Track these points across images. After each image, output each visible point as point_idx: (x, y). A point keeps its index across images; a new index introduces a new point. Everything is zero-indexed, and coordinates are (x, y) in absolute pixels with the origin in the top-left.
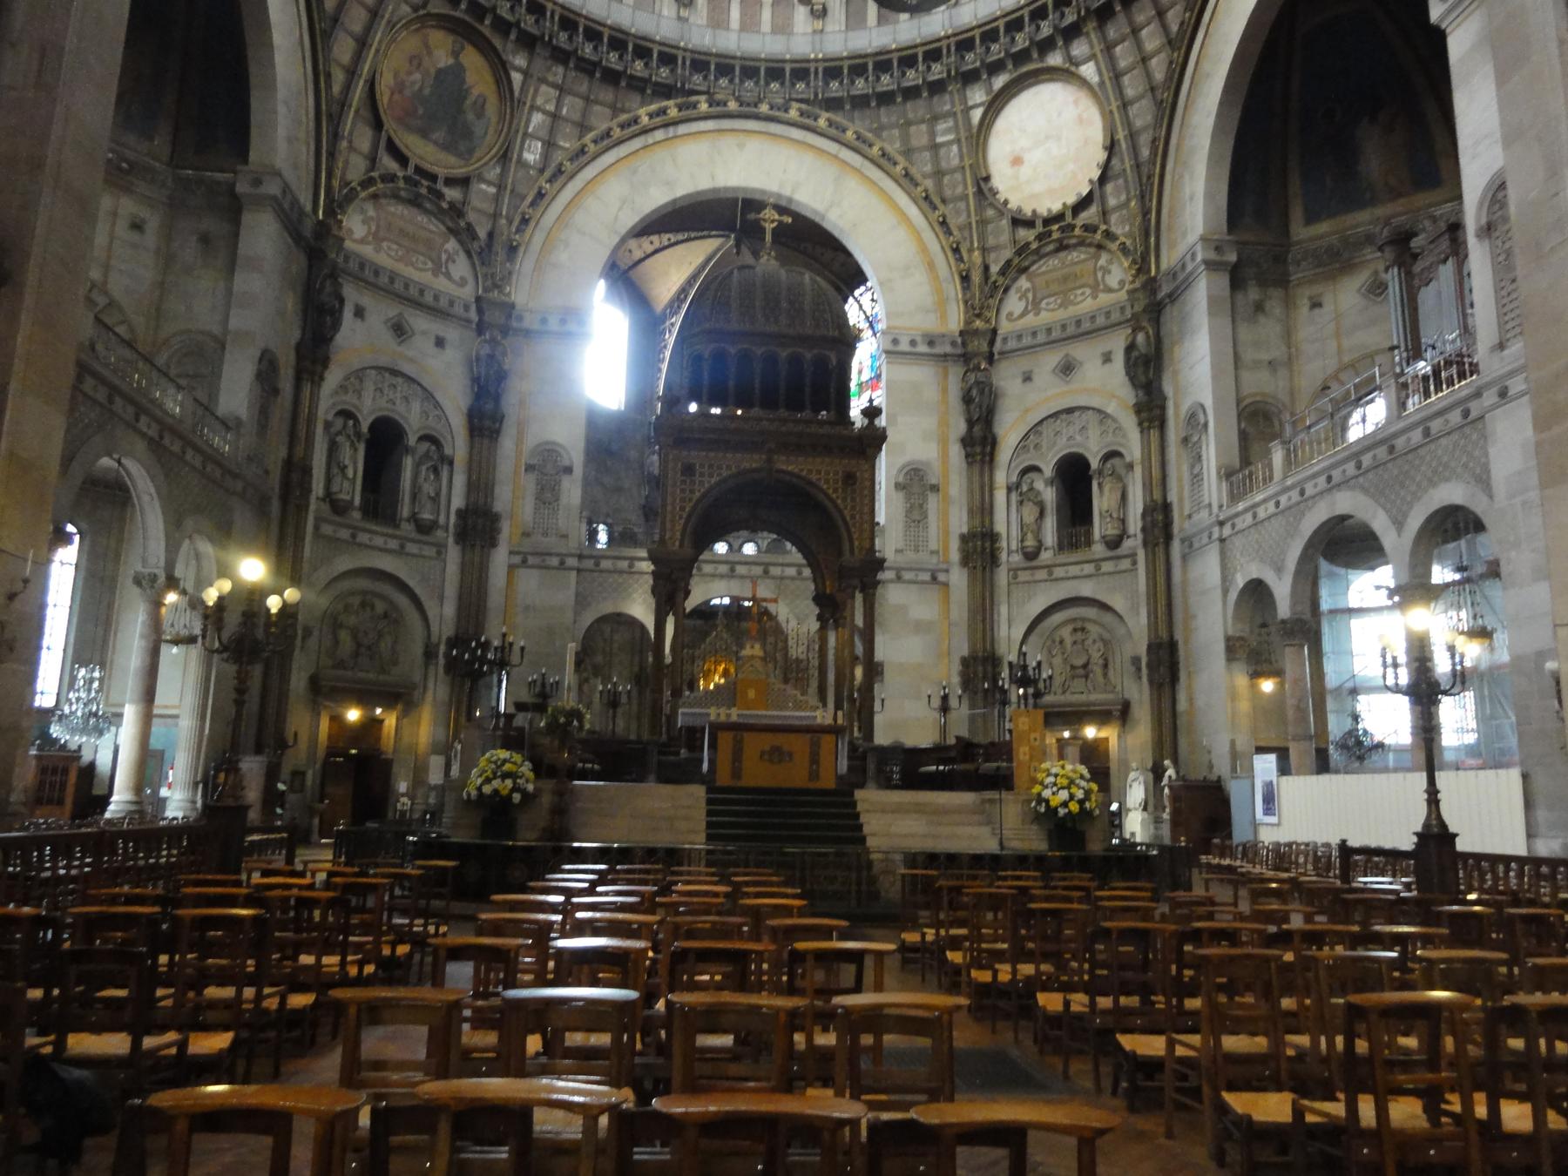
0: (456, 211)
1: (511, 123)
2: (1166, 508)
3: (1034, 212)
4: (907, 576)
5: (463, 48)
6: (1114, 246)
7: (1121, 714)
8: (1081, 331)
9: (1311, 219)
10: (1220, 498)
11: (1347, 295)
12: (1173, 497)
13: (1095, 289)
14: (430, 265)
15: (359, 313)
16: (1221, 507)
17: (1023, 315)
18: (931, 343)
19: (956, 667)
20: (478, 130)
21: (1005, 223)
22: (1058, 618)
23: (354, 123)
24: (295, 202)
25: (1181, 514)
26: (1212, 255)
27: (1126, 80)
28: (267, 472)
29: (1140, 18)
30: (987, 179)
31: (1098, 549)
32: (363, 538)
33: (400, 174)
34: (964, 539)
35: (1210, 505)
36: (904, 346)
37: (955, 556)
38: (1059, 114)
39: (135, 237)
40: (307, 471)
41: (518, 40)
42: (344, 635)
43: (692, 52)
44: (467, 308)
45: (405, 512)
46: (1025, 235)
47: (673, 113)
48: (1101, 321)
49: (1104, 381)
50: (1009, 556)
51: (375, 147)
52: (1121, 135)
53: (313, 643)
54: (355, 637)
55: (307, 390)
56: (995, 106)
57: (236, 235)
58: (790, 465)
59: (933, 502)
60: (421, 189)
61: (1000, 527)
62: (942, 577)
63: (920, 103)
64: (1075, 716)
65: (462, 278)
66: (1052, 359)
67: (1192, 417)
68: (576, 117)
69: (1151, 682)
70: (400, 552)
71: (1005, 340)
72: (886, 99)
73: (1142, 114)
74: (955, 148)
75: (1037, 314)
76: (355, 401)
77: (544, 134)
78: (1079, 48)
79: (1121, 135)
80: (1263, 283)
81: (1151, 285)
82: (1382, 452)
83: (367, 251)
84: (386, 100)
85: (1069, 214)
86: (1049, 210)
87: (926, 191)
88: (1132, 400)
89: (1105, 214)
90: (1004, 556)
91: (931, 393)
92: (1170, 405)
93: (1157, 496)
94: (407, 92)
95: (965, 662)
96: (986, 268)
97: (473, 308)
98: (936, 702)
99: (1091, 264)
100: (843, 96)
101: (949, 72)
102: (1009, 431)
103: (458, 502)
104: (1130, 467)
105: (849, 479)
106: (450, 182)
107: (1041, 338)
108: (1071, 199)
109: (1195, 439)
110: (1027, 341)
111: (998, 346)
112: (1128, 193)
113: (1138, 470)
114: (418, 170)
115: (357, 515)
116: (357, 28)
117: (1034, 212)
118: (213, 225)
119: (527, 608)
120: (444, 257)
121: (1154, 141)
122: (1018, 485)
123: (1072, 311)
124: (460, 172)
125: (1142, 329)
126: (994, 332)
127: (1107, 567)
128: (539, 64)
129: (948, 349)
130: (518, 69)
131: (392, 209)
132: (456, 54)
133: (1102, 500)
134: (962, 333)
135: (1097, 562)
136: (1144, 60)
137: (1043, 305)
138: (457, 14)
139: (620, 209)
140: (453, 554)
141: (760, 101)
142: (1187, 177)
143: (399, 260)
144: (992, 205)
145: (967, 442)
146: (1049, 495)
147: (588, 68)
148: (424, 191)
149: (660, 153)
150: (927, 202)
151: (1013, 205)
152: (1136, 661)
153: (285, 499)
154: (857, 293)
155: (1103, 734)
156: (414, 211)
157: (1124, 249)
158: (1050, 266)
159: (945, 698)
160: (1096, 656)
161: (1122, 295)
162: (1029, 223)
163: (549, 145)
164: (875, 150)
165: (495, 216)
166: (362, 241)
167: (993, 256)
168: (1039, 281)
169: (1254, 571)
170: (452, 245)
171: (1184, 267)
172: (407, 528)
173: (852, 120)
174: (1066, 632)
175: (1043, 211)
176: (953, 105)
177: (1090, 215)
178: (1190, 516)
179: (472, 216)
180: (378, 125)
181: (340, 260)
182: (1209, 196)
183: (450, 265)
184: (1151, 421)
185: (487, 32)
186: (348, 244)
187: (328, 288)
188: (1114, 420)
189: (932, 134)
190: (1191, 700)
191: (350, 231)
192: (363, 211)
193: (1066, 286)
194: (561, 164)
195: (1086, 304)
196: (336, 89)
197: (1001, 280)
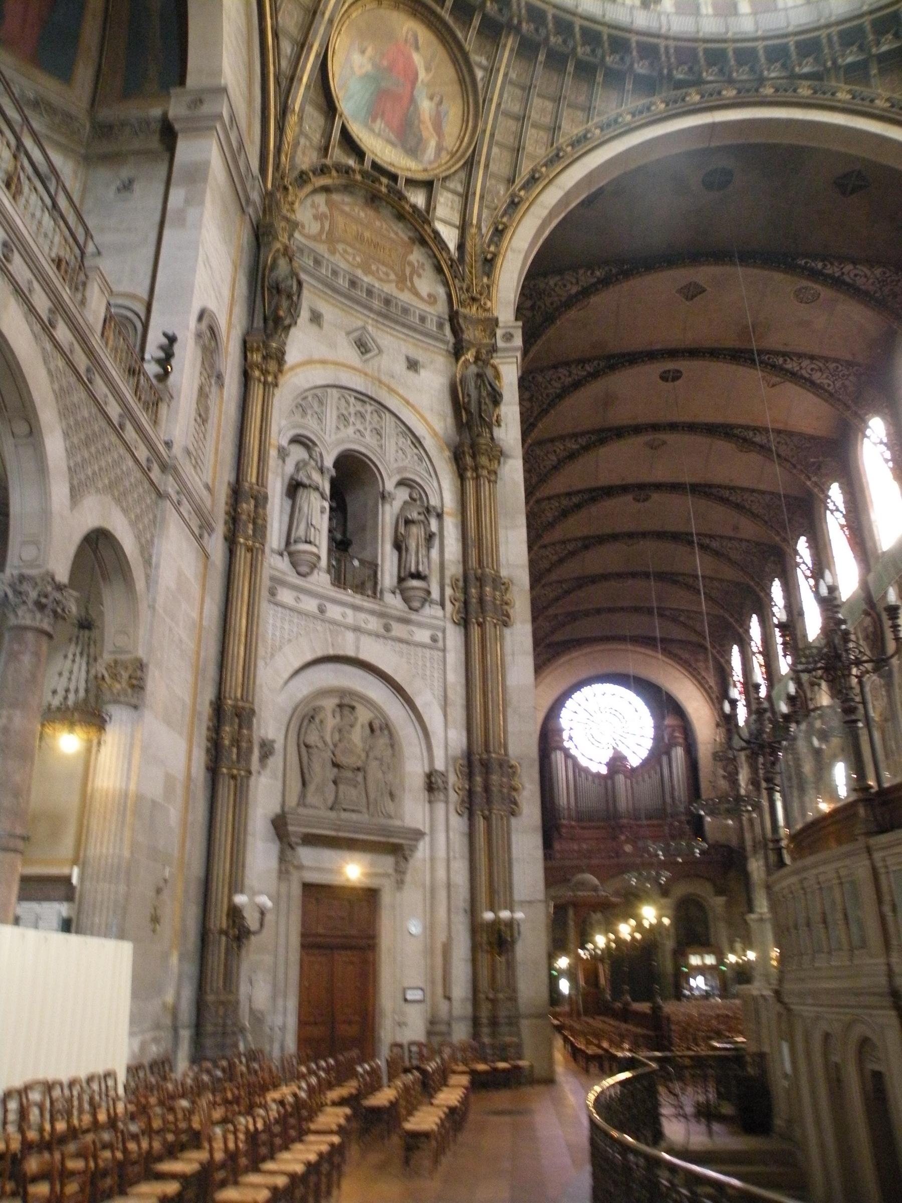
14: (393, 277)
15: (316, 318)
40: (261, 500)
43: (675, 39)
44: (440, 326)
55: (257, 391)
103: (454, 569)
114: (375, 165)
120: (408, 270)
130: (480, 66)
140: (454, 638)
143: (358, 266)
148: (384, 190)
183: (415, 278)
185: (447, 17)
186: (297, 235)
194: (534, 171)
196: (284, 64)
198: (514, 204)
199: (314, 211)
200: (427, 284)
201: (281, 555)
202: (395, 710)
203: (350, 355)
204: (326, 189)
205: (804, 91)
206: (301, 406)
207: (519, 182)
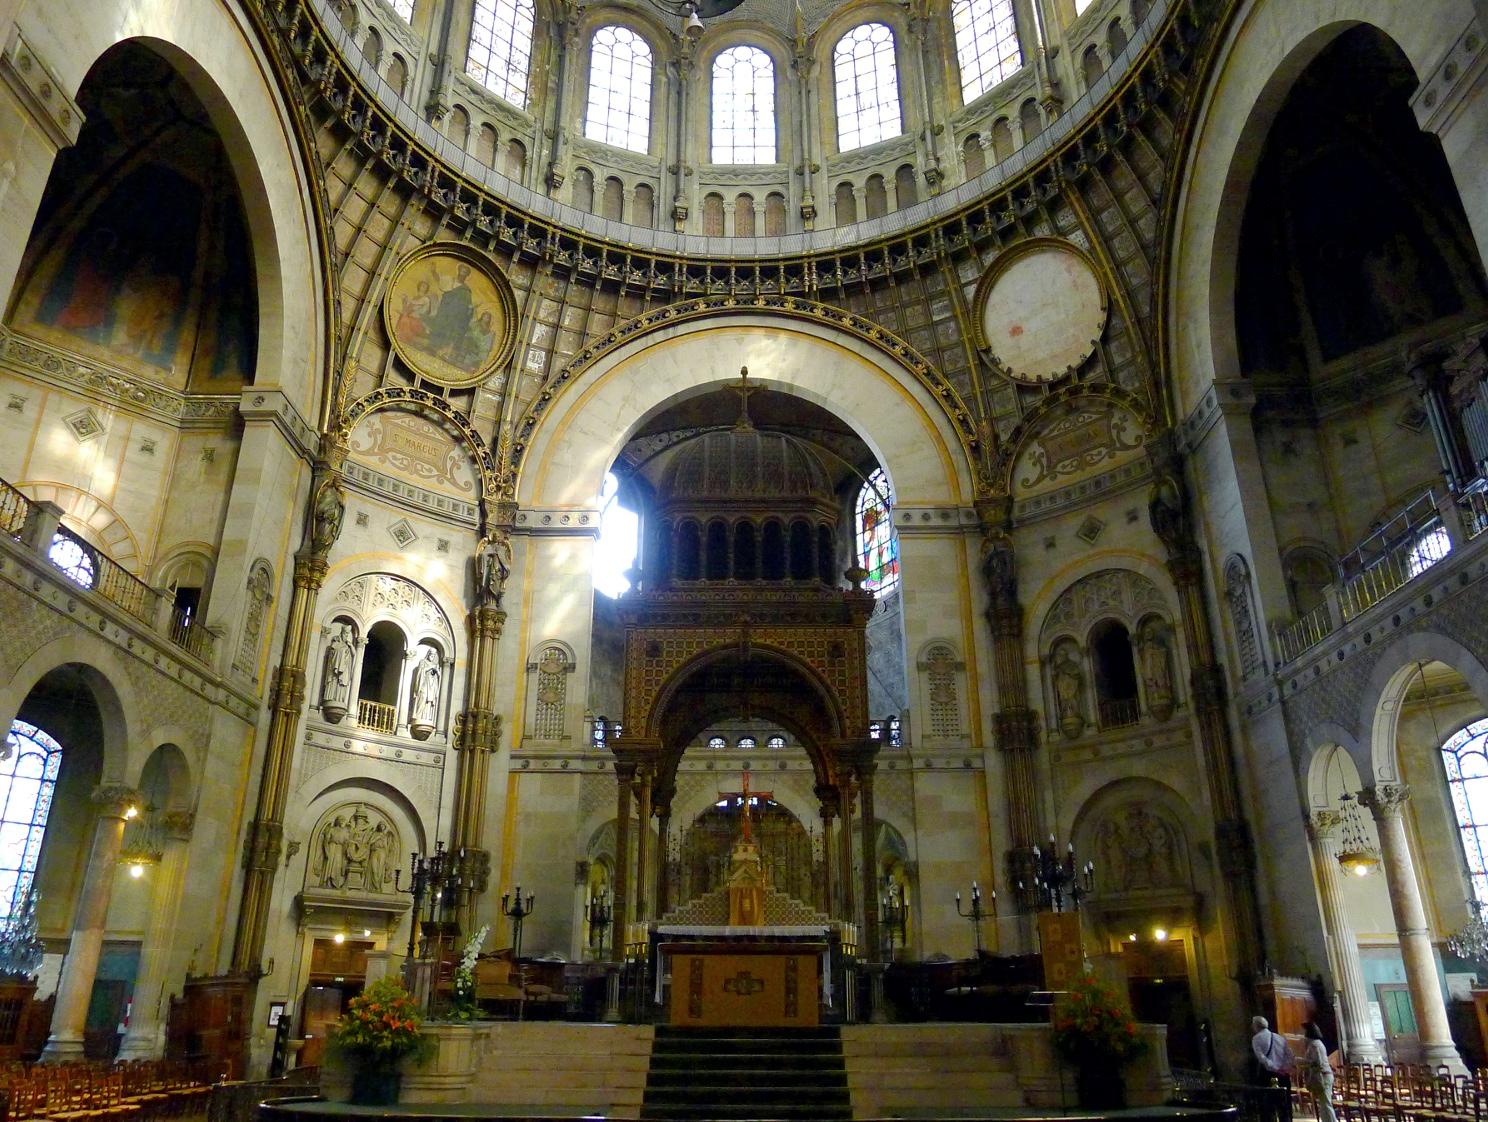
0: (462, 420)
1: (515, 335)
2: (1216, 670)
3: (1039, 377)
4: (938, 763)
5: (468, 273)
6: (1126, 403)
8: (1102, 490)
9: (1327, 358)
10: (1275, 655)
11: (1383, 428)
12: (1223, 659)
13: (1111, 447)
14: (435, 472)
15: (362, 520)
16: (1277, 665)
17: (1039, 480)
18: (945, 516)
19: (1000, 865)
20: (484, 345)
21: (1011, 391)
23: (362, 343)
24: (297, 417)
25: (1233, 675)
26: (1230, 399)
27: (1116, 243)
28: (254, 680)
29: (1122, 184)
30: (988, 350)
31: (1146, 721)
33: (407, 389)
34: (999, 719)
35: (1265, 662)
36: (917, 521)
37: (989, 738)
38: (1054, 282)
39: (145, 457)
40: (298, 677)
41: (520, 262)
42: (335, 852)
44: (470, 511)
46: (1030, 400)
47: (673, 315)
49: (1132, 540)
50: (1048, 737)
51: (383, 368)
52: (1118, 295)
53: (299, 859)
54: (345, 854)
55: (303, 594)
56: (987, 282)
57: (236, 452)
58: (766, 639)
59: (961, 682)
60: (427, 400)
61: (1037, 704)
62: (977, 763)
65: (466, 483)
66: (1074, 522)
67: (1232, 567)
68: (576, 327)
69: (1222, 866)
71: (1023, 507)
73: (1138, 272)
74: (952, 324)
75: (1054, 478)
76: (354, 606)
77: (545, 345)
78: (1065, 219)
79: (1118, 295)
80: (1286, 424)
81: (1170, 438)
82: (1452, 582)
83: (372, 461)
84: (394, 322)
85: (1075, 375)
86: (1054, 375)
87: (927, 368)
89: (1112, 372)
90: (1043, 736)
91: (949, 568)
92: (1207, 557)
93: (1205, 657)
94: (415, 315)
96: (996, 437)
97: (477, 510)
98: (967, 908)
99: (1105, 422)
101: (939, 254)
104: (1171, 629)
105: (836, 650)
106: (454, 393)
108: (1076, 362)
109: (1238, 592)
110: (1046, 506)
111: (1016, 513)
112: (1133, 350)
113: (1181, 635)
116: (368, 262)
117: (1039, 377)
118: (218, 443)
119: (528, 816)
121: (1152, 295)
122: (1051, 657)
123: (1090, 472)
124: (464, 385)
125: (1166, 482)
126: (1010, 499)
127: (1158, 741)
129: (964, 521)
131: (399, 421)
132: (462, 279)
133: (1145, 667)
134: (976, 504)
136: (1132, 222)
137: (1059, 468)
138: (464, 243)
139: (622, 408)
140: (452, 757)
142: (1191, 326)
143: (405, 468)
145: (992, 616)
146: (1087, 666)
148: (429, 403)
149: (660, 353)
151: (1017, 373)
153: (274, 708)
154: (871, 478)
155: (1176, 936)
156: (421, 421)
157: (1136, 405)
158: (1060, 428)
159: (976, 901)
160: (1158, 845)
161: (1141, 451)
163: (551, 353)
165: (498, 423)
166: (369, 452)
167: (1001, 425)
170: (456, 452)
171: (1200, 413)
172: (405, 734)
173: (849, 309)
175: (1048, 376)
176: (947, 285)
177: (1096, 374)
178: (1244, 678)
179: (475, 424)
180: (386, 345)
181: (344, 471)
182: (1217, 342)
184: (1186, 576)
186: (352, 455)
187: (330, 495)
188: (1148, 581)
189: (928, 314)
190: (1273, 893)
191: (356, 444)
193: (1080, 448)
196: (347, 316)
197: (1012, 447)
198: (545, 400)
199: (369, 429)
200: (465, 474)
201: (318, 709)
205: (789, 307)
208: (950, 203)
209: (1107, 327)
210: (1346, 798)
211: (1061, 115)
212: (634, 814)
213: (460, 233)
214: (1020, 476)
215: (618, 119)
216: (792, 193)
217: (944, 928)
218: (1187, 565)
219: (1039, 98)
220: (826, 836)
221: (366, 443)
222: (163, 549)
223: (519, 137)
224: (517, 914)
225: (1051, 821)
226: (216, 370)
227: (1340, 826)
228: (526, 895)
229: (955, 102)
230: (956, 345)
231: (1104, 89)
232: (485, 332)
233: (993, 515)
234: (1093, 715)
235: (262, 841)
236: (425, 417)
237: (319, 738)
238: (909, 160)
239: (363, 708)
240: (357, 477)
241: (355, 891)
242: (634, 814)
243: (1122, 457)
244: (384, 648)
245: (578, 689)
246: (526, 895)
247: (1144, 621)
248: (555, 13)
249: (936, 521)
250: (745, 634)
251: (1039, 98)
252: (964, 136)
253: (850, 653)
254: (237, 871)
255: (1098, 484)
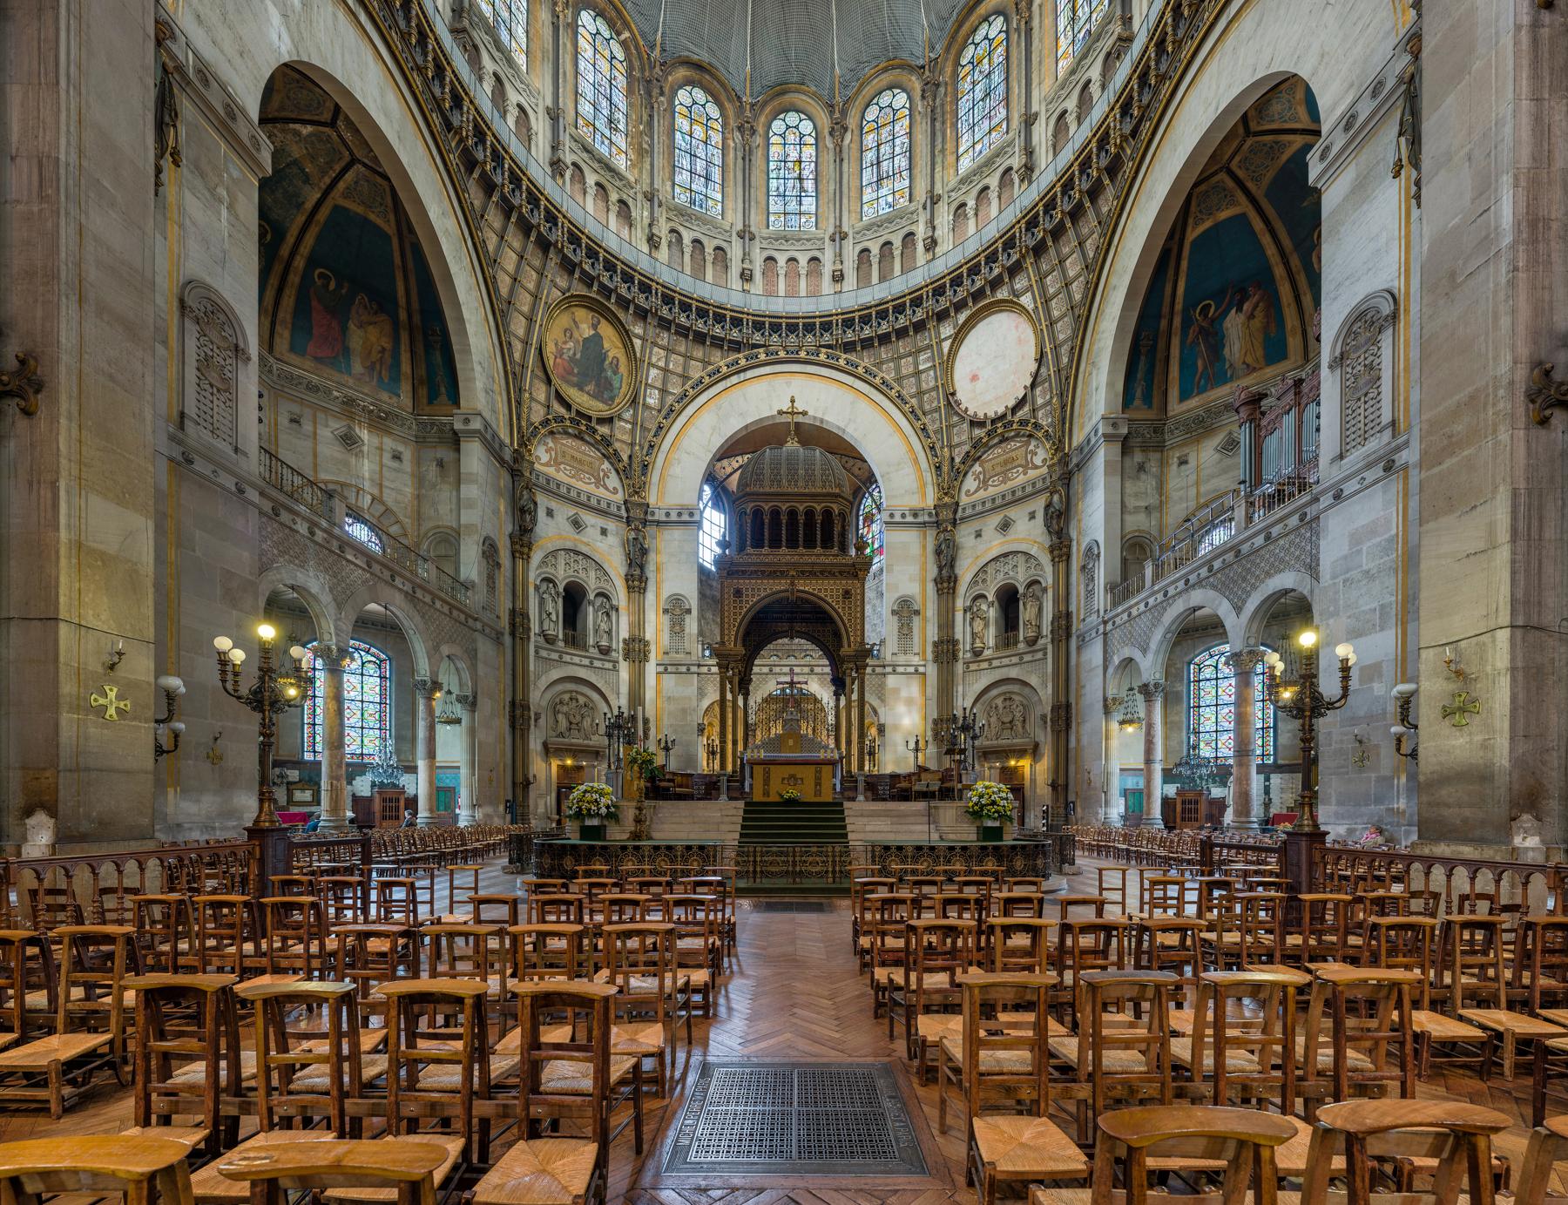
7: (1035, 752)
8: (1016, 499)
13: (1027, 466)
15: (550, 513)
19: (930, 725)
22: (994, 692)
31: (1021, 646)
32: (567, 658)
42: (560, 717)
45: (591, 641)
48: (1029, 489)
49: (1029, 532)
50: (964, 654)
51: (548, 398)
53: (542, 721)
60: (583, 426)
63: (908, 340)
64: (1005, 753)
66: (995, 520)
70: (591, 666)
72: (884, 339)
83: (551, 471)
88: (1047, 544)
95: (935, 722)
100: (853, 339)
102: (966, 570)
104: (1045, 590)
106: (601, 421)
107: (988, 505)
108: (1011, 403)
114: (578, 412)
115: (561, 644)
123: (1010, 484)
124: (606, 414)
127: (1027, 658)
128: (651, 331)
132: (595, 327)
133: (1026, 613)
135: (1020, 655)
141: (801, 348)
144: (957, 414)
147: (683, 332)
150: (913, 415)
152: (1044, 717)
158: (995, 455)
162: (981, 424)
164: (878, 381)
166: (547, 464)
168: (988, 466)
169: (1127, 652)
174: (999, 702)
175: (991, 415)
192: (546, 444)
195: (1019, 479)
202: (595, 696)
203: (568, 529)
204: (552, 433)
206: (543, 562)
207: (664, 412)
208: (941, 267)
209: (1036, 376)
210: (1131, 689)
211: (1030, 183)
212: (729, 696)
213: (590, 286)
214: (965, 488)
215: (699, 185)
216: (828, 258)
217: (895, 758)
218: (1060, 547)
219: (1016, 167)
220: (837, 706)
221: (545, 458)
222: (423, 530)
223: (625, 197)
224: (667, 749)
225: (960, 702)
226: (432, 398)
227: (1122, 708)
228: (670, 739)
229: (952, 171)
230: (932, 389)
231: (1067, 155)
232: (615, 373)
233: (946, 514)
234: (992, 642)
235: (518, 712)
236: (582, 439)
237: (544, 653)
238: (913, 228)
239: (565, 635)
240: (542, 481)
241: (576, 740)
242: (729, 696)
243: (1032, 474)
244: (573, 598)
245: (692, 625)
246: (670, 739)
247: (1030, 585)
248: (642, 70)
249: (909, 519)
250: (792, 584)
251: (1016, 167)
252: (954, 205)
253: (853, 597)
254: (507, 729)
255: (1014, 493)
